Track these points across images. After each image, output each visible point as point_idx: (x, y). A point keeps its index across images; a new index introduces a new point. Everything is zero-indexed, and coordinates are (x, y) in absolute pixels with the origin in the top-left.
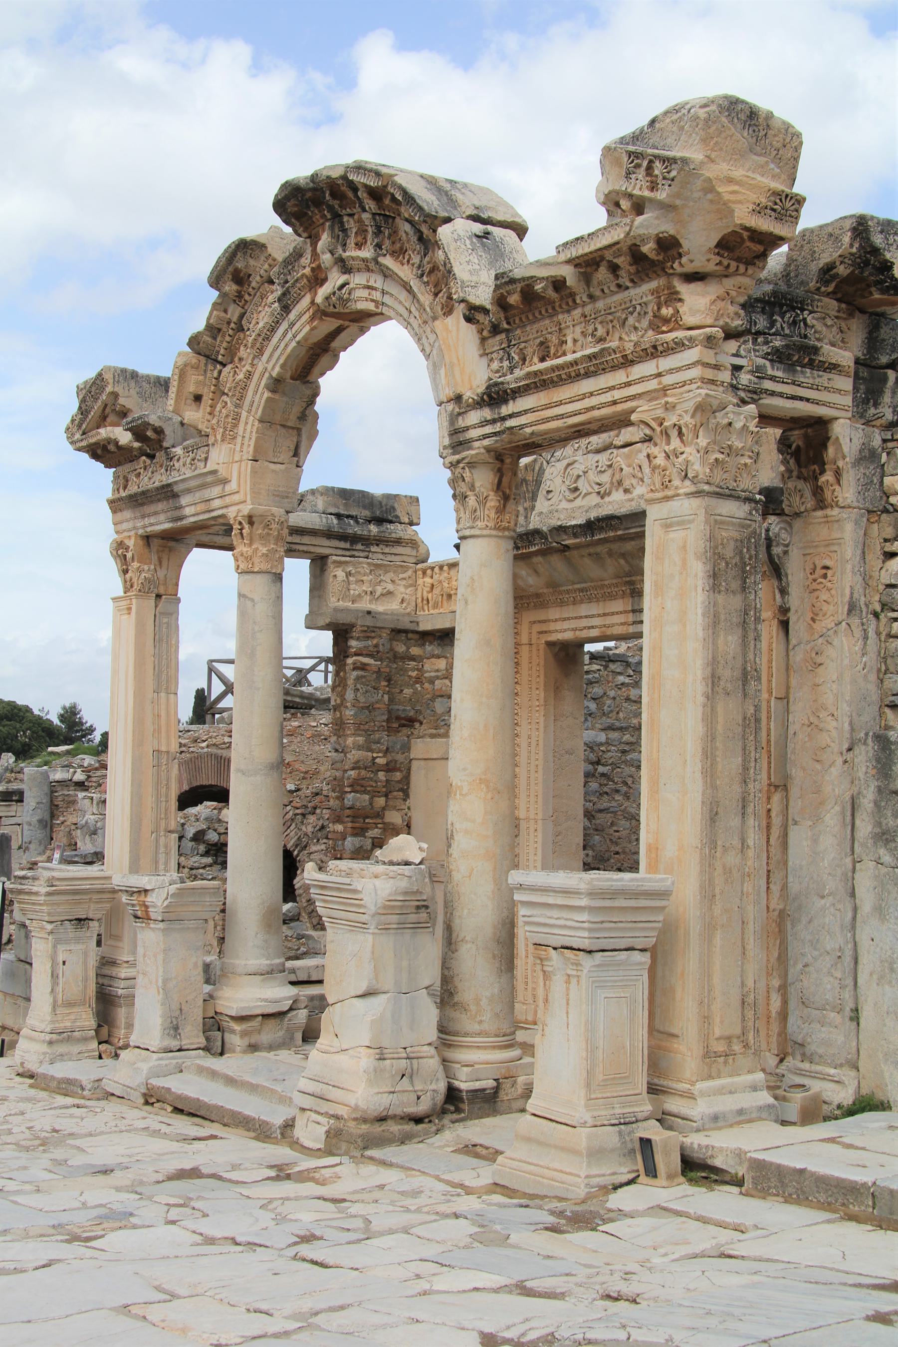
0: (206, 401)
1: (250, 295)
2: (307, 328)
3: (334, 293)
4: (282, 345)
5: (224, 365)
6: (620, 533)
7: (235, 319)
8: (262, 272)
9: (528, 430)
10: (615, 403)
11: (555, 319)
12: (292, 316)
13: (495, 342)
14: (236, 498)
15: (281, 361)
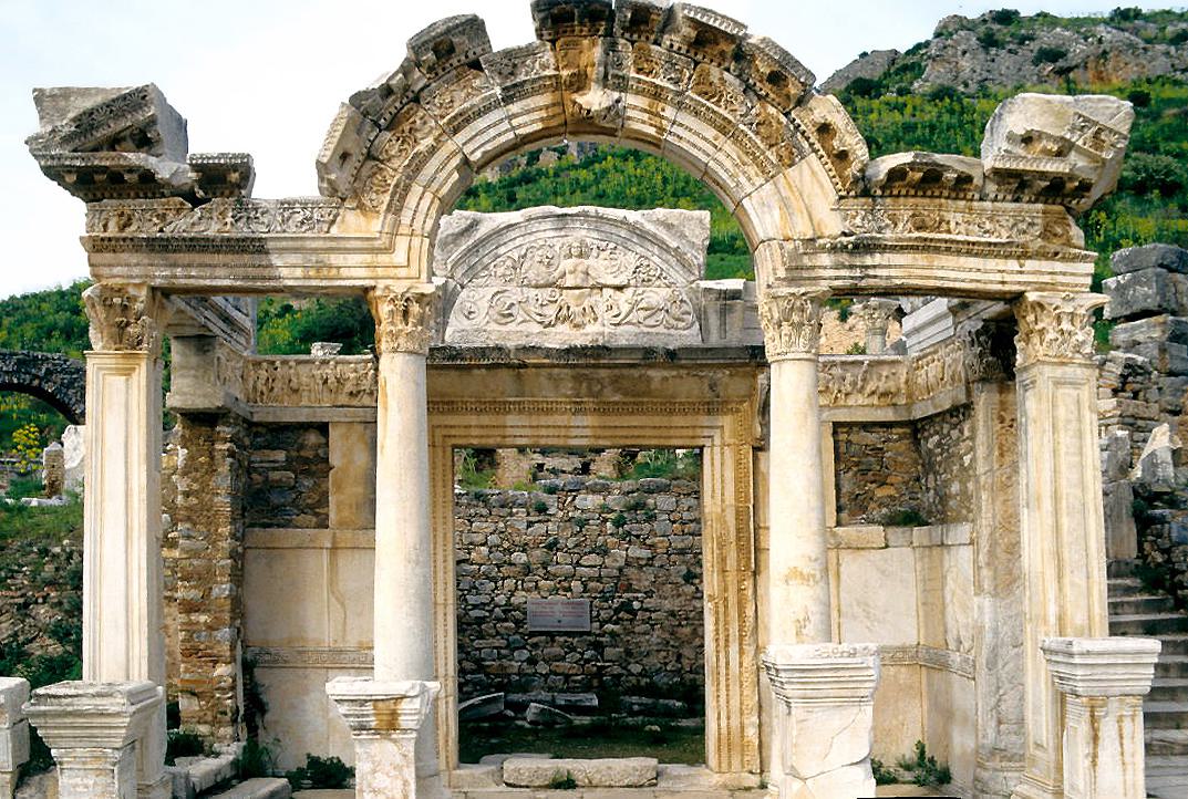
0: (353, 162)
1: (444, 69)
2: (539, 126)
3: (613, 106)
4: (492, 132)
5: (380, 131)
6: (606, 361)
7: (417, 88)
8: (471, 55)
9: (898, 282)
10: (1003, 283)
11: (937, 201)
12: (514, 108)
13: (857, 205)
14: (403, 272)
15: (488, 147)
